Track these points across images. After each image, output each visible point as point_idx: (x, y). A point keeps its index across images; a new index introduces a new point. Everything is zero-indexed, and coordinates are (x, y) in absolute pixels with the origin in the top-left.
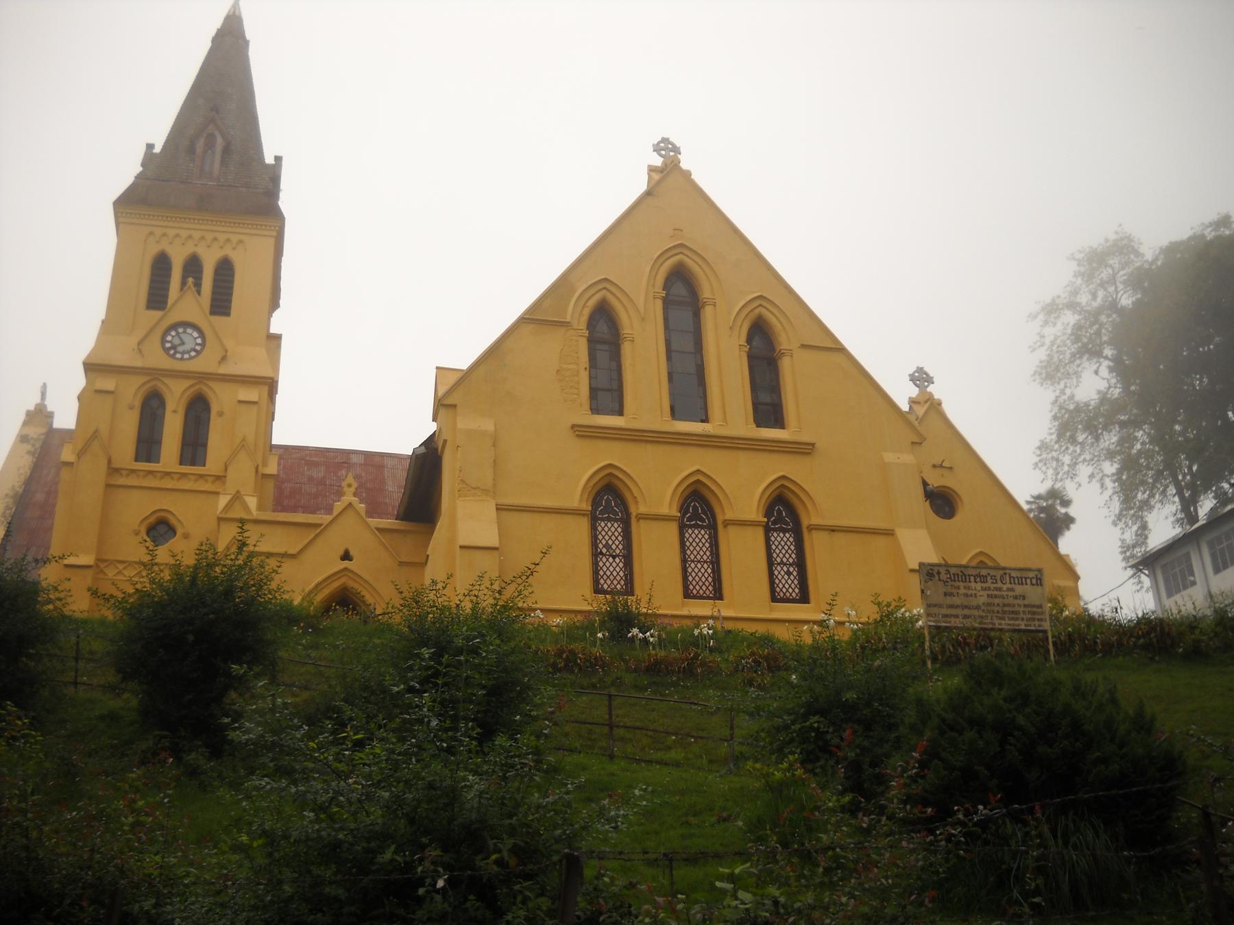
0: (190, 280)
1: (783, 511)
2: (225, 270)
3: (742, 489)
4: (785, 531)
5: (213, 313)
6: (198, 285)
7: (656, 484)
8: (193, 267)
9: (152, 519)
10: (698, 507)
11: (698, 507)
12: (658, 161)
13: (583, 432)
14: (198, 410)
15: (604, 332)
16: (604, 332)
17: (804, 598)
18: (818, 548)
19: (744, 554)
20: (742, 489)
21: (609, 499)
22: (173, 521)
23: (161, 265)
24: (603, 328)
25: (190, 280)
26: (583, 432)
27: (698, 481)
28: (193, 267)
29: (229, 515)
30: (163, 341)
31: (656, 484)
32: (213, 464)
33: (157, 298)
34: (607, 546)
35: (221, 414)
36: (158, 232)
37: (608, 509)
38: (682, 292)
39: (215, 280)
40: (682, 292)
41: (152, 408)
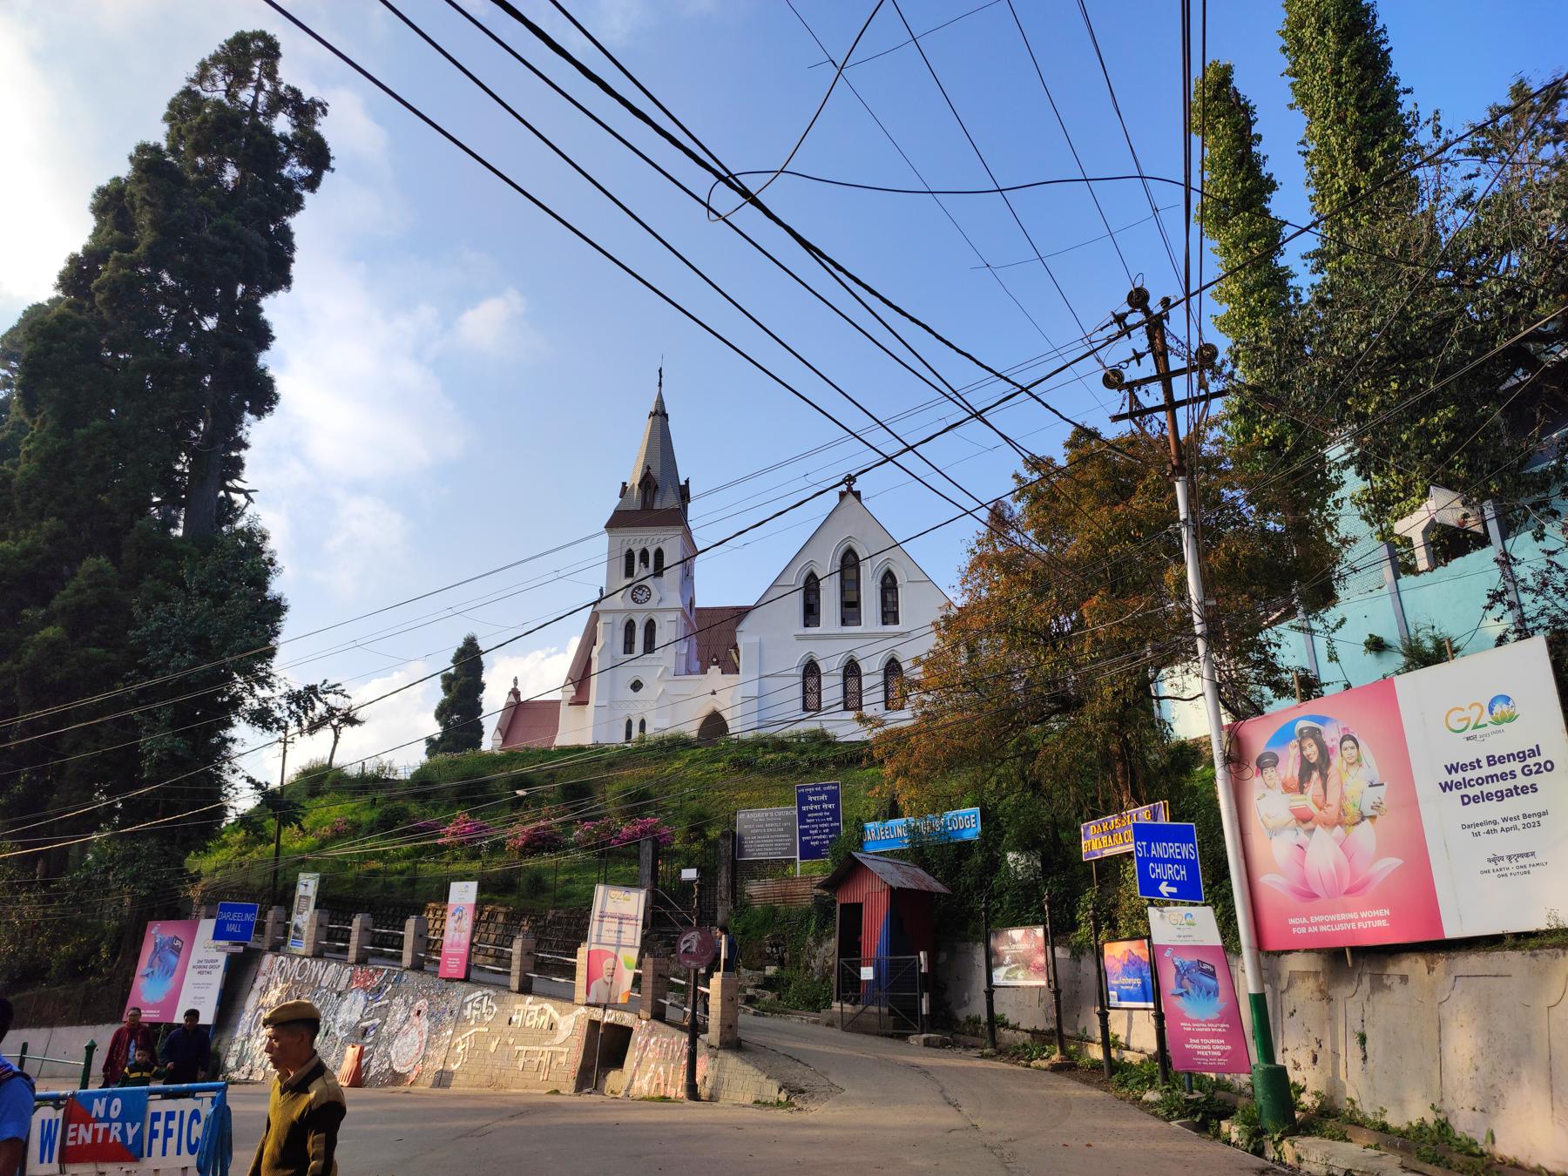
13: (799, 637)
15: (811, 586)
16: (811, 586)
21: (811, 670)
26: (799, 637)
38: (849, 562)
40: (849, 562)
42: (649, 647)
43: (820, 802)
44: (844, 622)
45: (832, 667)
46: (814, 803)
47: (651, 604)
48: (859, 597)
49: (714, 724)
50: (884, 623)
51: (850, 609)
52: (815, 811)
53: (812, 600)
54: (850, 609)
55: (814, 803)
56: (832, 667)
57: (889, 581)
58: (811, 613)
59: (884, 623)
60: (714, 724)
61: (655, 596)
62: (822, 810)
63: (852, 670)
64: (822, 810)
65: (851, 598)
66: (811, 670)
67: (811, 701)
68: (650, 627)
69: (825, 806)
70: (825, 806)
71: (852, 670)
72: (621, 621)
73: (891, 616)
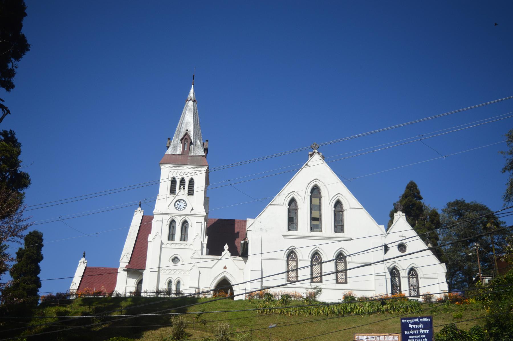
0: (182, 186)
1: (340, 257)
2: (192, 181)
3: (328, 253)
4: (342, 263)
5: (188, 195)
6: (184, 189)
8: (182, 181)
9: (173, 257)
10: (316, 256)
11: (316, 256)
17: (346, 282)
20: (328, 253)
21: (291, 255)
22: (179, 257)
23: (173, 181)
25: (182, 186)
26: (285, 237)
27: (317, 250)
28: (182, 181)
29: (194, 257)
30: (175, 205)
33: (173, 191)
34: (291, 268)
35: (183, 285)
36: (172, 171)
37: (292, 258)
39: (189, 185)
42: (184, 236)
43: (418, 329)
44: (312, 229)
45: (304, 256)
46: (414, 329)
47: (187, 211)
48: (320, 216)
49: (224, 286)
50: (335, 232)
51: (316, 222)
52: (414, 334)
53: (292, 215)
54: (316, 222)
55: (414, 329)
56: (304, 256)
58: (292, 221)
59: (335, 232)
60: (224, 286)
61: (189, 208)
62: (420, 334)
64: (420, 334)
65: (316, 215)
67: (291, 273)
68: (185, 224)
69: (422, 331)
70: (422, 331)
72: (166, 220)
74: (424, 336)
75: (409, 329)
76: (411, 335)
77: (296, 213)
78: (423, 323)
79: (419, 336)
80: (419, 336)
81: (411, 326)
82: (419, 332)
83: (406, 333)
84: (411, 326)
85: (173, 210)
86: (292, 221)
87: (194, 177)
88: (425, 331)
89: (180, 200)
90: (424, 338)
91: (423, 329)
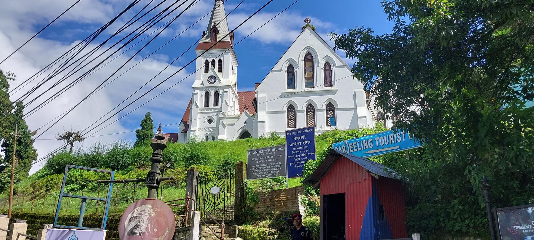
2: (220, 62)
3: (320, 103)
7: (301, 104)
8: (213, 62)
12: (305, 24)
14: (216, 94)
18: (338, 113)
19: (321, 118)
20: (320, 103)
23: (207, 62)
24: (291, 70)
31: (301, 104)
32: (219, 106)
33: (207, 71)
41: (207, 95)
43: (301, 140)
46: (297, 141)
51: (310, 81)
52: (298, 146)
53: (291, 77)
54: (310, 81)
55: (297, 141)
57: (327, 67)
58: (291, 83)
62: (303, 145)
63: (311, 108)
64: (303, 145)
66: (291, 109)
69: (304, 142)
70: (304, 142)
71: (311, 108)
73: (328, 83)
74: (306, 147)
75: (294, 141)
76: (295, 147)
77: (294, 75)
78: (305, 134)
79: (302, 148)
80: (302, 148)
81: (295, 138)
82: (302, 143)
83: (291, 145)
84: (295, 138)
85: (207, 84)
86: (291, 83)
87: (222, 59)
88: (308, 142)
89: (211, 77)
90: (307, 149)
91: (306, 140)
